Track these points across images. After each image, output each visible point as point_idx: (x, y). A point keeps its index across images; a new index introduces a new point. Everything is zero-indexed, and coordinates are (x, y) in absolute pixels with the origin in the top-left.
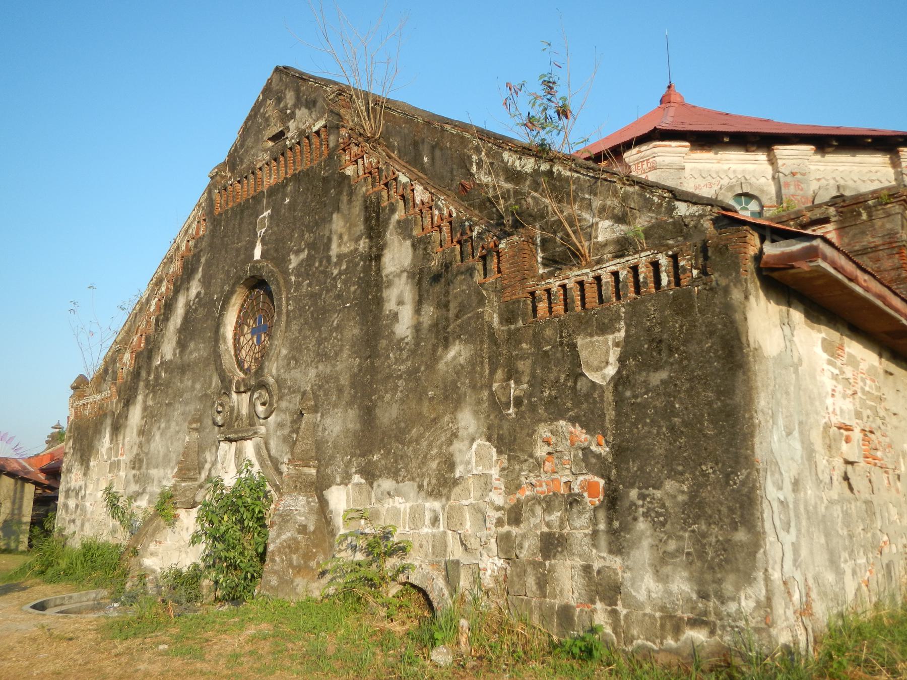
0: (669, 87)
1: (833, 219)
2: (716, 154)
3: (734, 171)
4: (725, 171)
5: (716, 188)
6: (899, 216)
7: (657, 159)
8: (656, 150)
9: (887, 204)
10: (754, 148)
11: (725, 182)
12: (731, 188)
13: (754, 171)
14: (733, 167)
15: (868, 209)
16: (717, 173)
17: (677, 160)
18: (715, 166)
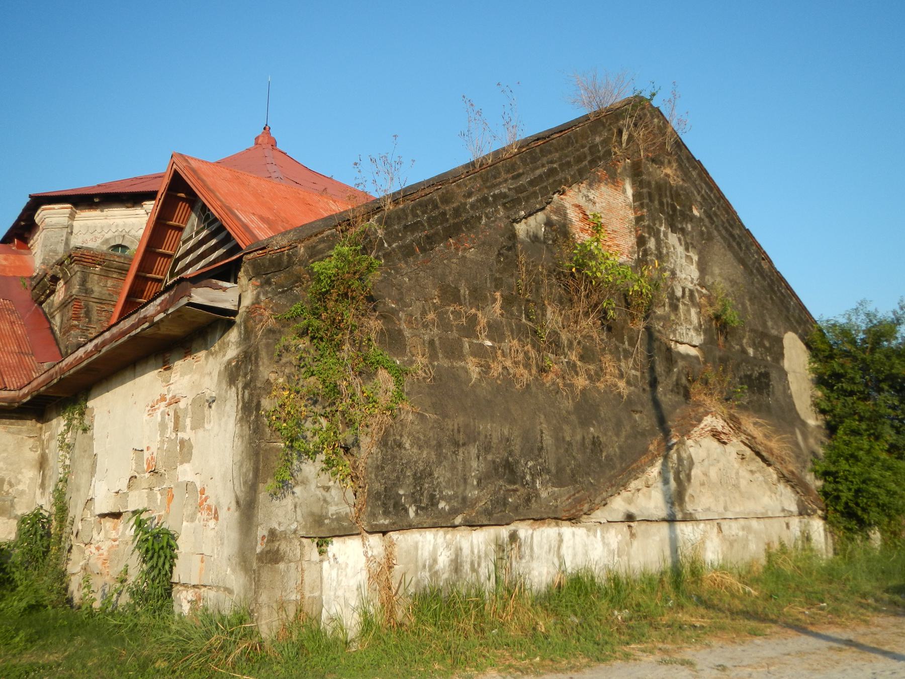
0: (265, 129)
1: (61, 276)
2: (102, 211)
3: (117, 226)
4: (110, 226)
5: (99, 241)
6: (79, 274)
7: (47, 220)
8: (44, 213)
9: (71, 263)
10: (129, 205)
11: (107, 236)
12: (107, 241)
13: (133, 224)
14: (119, 221)
15: (67, 267)
16: (102, 228)
17: (64, 220)
18: (104, 222)
